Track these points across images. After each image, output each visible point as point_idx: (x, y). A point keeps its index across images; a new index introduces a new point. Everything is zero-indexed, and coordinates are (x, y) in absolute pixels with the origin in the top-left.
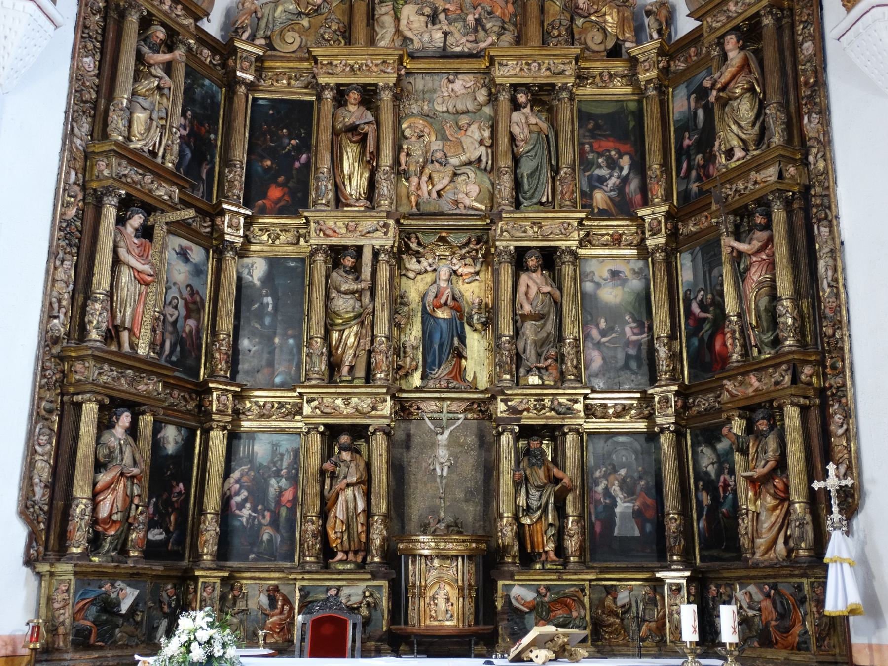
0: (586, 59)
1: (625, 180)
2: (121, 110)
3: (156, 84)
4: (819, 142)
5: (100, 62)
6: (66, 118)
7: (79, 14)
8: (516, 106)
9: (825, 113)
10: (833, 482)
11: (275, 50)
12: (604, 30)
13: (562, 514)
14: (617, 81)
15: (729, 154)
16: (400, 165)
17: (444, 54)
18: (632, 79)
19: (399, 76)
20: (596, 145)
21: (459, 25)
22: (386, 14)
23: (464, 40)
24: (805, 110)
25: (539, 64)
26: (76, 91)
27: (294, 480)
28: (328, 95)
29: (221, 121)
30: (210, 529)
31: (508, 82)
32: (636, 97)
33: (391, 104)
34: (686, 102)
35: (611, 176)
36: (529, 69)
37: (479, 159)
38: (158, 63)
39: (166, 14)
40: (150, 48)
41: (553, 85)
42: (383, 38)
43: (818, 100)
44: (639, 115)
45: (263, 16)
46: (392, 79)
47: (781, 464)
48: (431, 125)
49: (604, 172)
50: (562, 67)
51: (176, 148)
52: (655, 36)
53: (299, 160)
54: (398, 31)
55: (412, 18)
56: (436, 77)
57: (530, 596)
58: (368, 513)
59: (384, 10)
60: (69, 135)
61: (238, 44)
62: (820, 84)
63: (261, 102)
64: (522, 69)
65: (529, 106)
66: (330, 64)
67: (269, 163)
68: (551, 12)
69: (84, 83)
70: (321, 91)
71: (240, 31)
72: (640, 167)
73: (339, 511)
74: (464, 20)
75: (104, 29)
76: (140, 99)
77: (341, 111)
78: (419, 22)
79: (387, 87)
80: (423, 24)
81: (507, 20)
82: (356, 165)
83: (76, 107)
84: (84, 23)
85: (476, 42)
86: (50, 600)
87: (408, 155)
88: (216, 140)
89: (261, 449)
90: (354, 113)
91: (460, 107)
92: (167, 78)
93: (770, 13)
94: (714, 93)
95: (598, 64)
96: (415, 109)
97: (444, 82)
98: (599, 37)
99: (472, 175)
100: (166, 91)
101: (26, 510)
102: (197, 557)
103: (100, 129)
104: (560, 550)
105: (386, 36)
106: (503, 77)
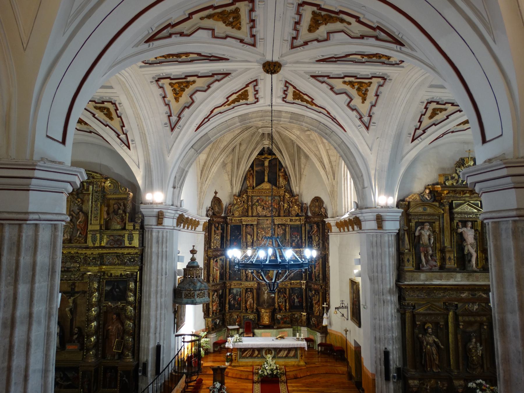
1: (298, 240)
10: (325, 306)
13: (286, 303)
27: (240, 296)
30: (227, 306)
47: (319, 300)
57: (280, 317)
58: (253, 303)
72: (301, 238)
73: (249, 303)
86: (208, 324)
89: (235, 291)
101: (203, 311)
102: (225, 311)
103: (210, 247)
104: (285, 309)
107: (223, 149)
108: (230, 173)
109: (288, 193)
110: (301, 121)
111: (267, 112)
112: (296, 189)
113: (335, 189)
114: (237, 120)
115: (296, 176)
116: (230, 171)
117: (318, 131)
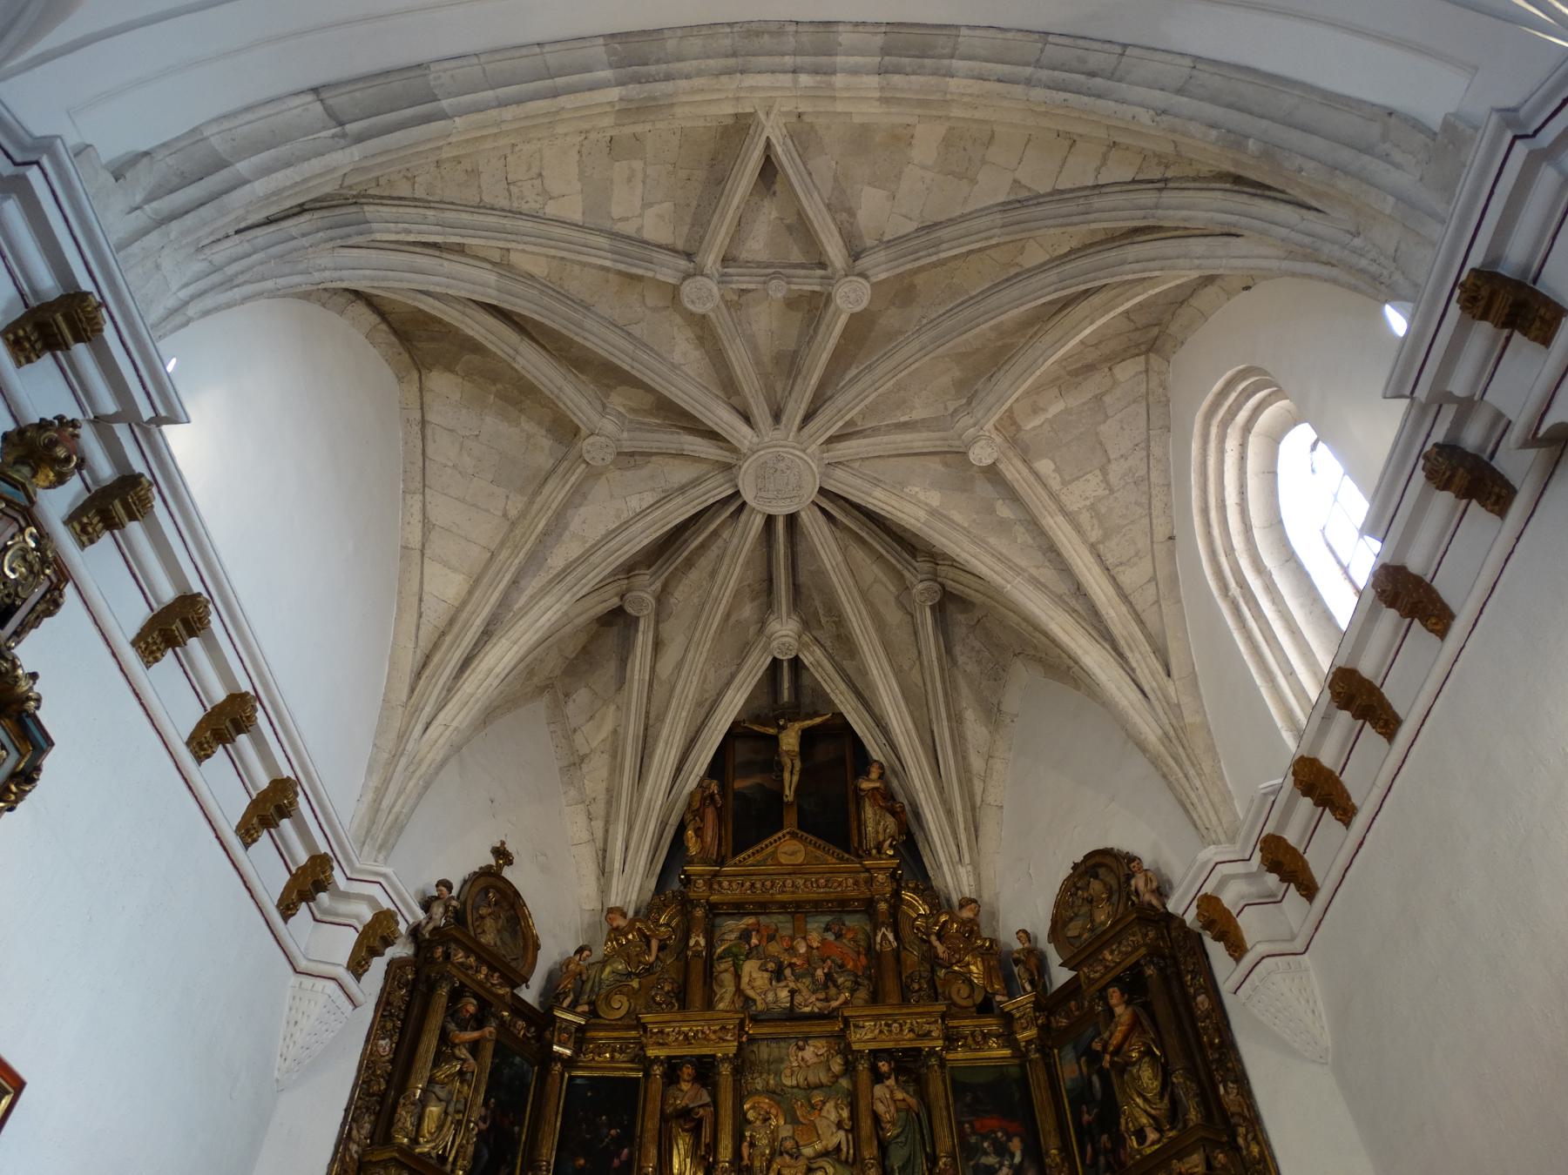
0: (954, 1017)
2: (413, 1104)
3: (458, 1067)
4: (1245, 1118)
5: (397, 1044)
6: (345, 1118)
7: (383, 990)
8: (878, 1078)
9: (1242, 1080)
11: (599, 1017)
12: (971, 982)
14: (993, 1042)
15: (1141, 1134)
16: (741, 1158)
17: (791, 1015)
18: (1008, 1039)
19: (740, 1044)
20: (977, 1125)
21: (807, 981)
22: (726, 971)
23: (813, 999)
24: (1218, 1077)
25: (901, 1025)
26: (364, 1082)
28: (657, 1070)
29: (529, 1109)
31: (867, 1048)
32: (1017, 1061)
33: (730, 1079)
34: (1076, 1067)
35: (1002, 1165)
36: (890, 1031)
37: (838, 1148)
38: (463, 1043)
39: (480, 983)
40: (457, 1025)
41: (919, 1050)
42: (721, 999)
43: (1230, 1065)
44: (1023, 1083)
45: (588, 978)
46: (732, 1048)
48: (778, 1104)
49: (991, 1160)
50: (927, 1027)
51: (471, 1149)
52: (1028, 988)
53: (619, 1156)
54: (739, 991)
55: (754, 975)
56: (782, 1044)
59: (723, 966)
60: (343, 1140)
61: (558, 1013)
62: (1228, 1046)
63: (578, 1081)
64: (881, 1032)
65: (893, 1077)
66: (661, 1032)
67: (582, 1162)
68: (908, 962)
69: (374, 1071)
70: (646, 1064)
71: (561, 997)
74: (813, 975)
75: (409, 1005)
76: (437, 1089)
77: (672, 1090)
78: (761, 979)
79: (726, 1058)
80: (767, 982)
81: (860, 974)
82: (688, 1160)
83: (360, 1102)
84: (388, 998)
85: (827, 1000)
87: (752, 1145)
88: (520, 1133)
90: (688, 1093)
91: (812, 1079)
92: (472, 1060)
93: (1152, 962)
94: (1107, 1057)
95: (967, 1022)
96: (759, 1084)
97: (793, 1049)
98: (965, 991)
99: (830, 1170)
100: (468, 1076)
105: (725, 999)
106: (860, 1041)
107: (558, 575)
108: (599, 809)
109: (914, 891)
110: (942, 57)
111: (758, 34)
112: (955, 874)
113: (1190, 718)
114: (599, 51)
115: (950, 813)
116: (602, 797)
117: (1044, 74)
